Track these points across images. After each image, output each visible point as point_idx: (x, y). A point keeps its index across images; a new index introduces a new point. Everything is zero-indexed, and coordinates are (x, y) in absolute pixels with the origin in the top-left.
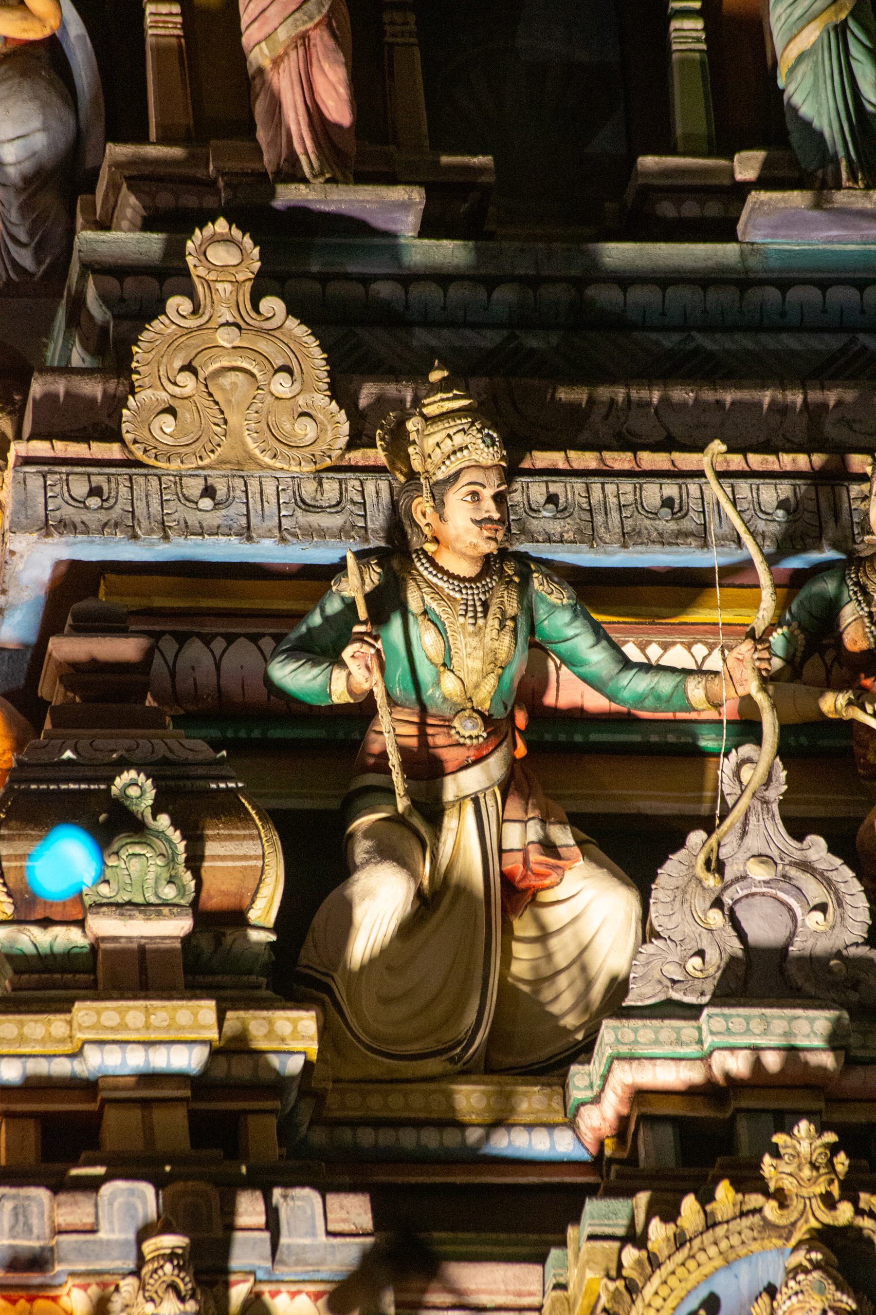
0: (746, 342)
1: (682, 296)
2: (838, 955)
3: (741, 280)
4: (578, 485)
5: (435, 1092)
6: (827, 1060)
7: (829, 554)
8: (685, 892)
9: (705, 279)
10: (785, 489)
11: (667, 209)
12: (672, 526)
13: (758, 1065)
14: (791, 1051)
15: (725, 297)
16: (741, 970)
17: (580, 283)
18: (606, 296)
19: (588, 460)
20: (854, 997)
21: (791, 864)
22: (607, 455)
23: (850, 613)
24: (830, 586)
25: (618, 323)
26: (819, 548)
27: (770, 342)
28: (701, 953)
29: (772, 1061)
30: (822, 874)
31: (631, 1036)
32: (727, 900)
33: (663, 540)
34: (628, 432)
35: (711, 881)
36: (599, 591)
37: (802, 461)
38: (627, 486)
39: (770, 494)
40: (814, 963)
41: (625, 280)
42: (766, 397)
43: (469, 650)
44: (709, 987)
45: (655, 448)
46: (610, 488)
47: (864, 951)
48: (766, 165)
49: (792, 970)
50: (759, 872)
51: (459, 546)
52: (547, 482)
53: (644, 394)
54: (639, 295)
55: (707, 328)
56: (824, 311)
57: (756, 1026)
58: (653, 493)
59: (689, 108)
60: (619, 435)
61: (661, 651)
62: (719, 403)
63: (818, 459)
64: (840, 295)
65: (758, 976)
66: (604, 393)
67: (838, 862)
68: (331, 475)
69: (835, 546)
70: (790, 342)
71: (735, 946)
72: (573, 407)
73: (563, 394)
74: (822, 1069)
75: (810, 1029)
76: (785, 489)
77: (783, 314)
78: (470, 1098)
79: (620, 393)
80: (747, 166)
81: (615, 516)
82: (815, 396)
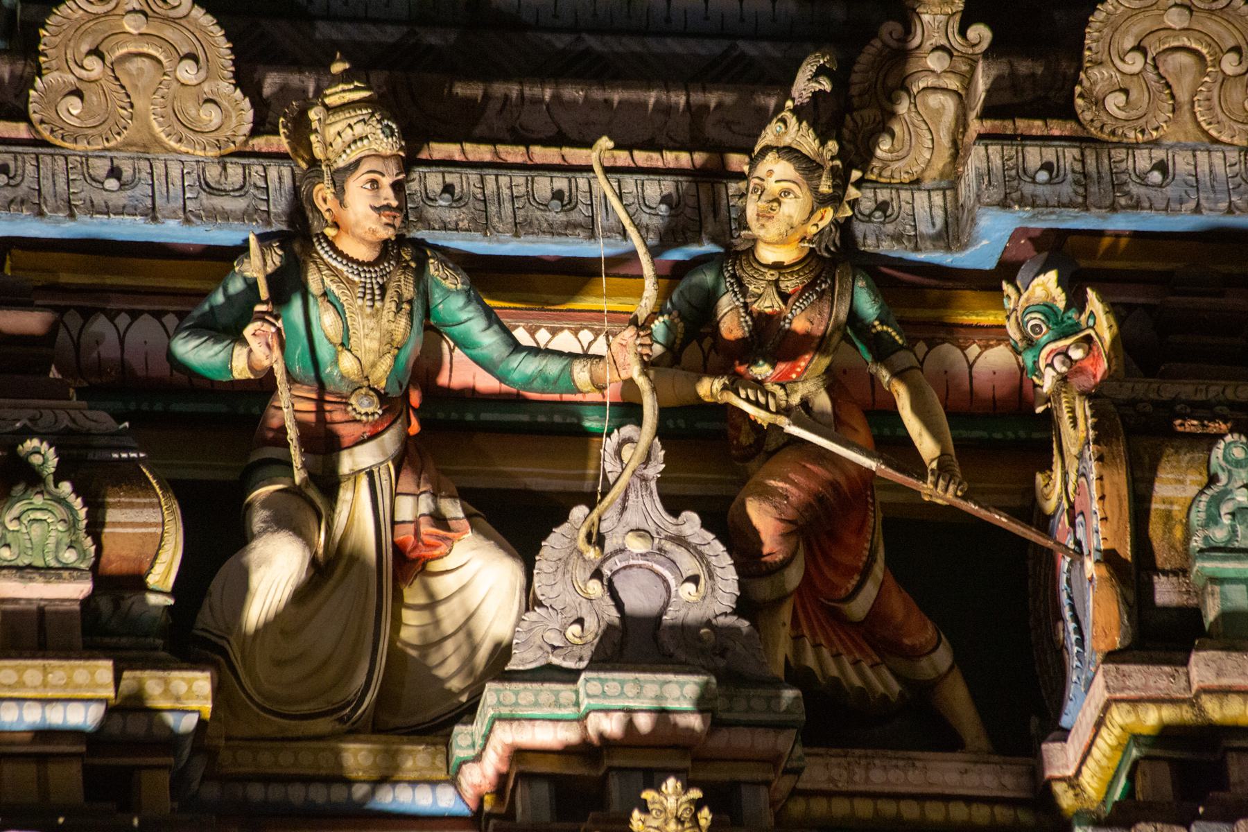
0: (633, 45)
2: (708, 624)
4: (474, 176)
5: (323, 750)
6: (695, 722)
7: (708, 248)
8: (566, 564)
10: (668, 185)
12: (562, 217)
13: (630, 726)
14: (662, 713)
16: (617, 637)
19: (482, 152)
20: (722, 663)
21: (666, 538)
22: (500, 148)
23: (726, 303)
24: (709, 278)
26: (699, 241)
28: (580, 621)
29: (644, 722)
30: (695, 548)
31: (511, 698)
32: (606, 572)
33: (553, 231)
34: (521, 126)
35: (592, 553)
36: (491, 278)
37: (684, 159)
38: (519, 179)
39: (654, 190)
40: (685, 631)
42: (652, 97)
43: (367, 331)
44: (587, 653)
45: (546, 143)
46: (504, 180)
47: (732, 620)
49: (665, 637)
50: (637, 546)
51: (359, 231)
52: (443, 173)
53: (537, 91)
57: (630, 690)
58: (544, 185)
60: (512, 130)
61: (549, 336)
62: (607, 102)
63: (699, 157)
65: (634, 643)
66: (498, 89)
67: (710, 536)
68: (235, 160)
69: (714, 240)
71: (613, 614)
72: (469, 102)
73: (460, 90)
74: (690, 730)
75: (680, 692)
76: (668, 185)
77: (668, 20)
78: (357, 756)
79: (514, 90)
81: (507, 206)
82: (697, 98)
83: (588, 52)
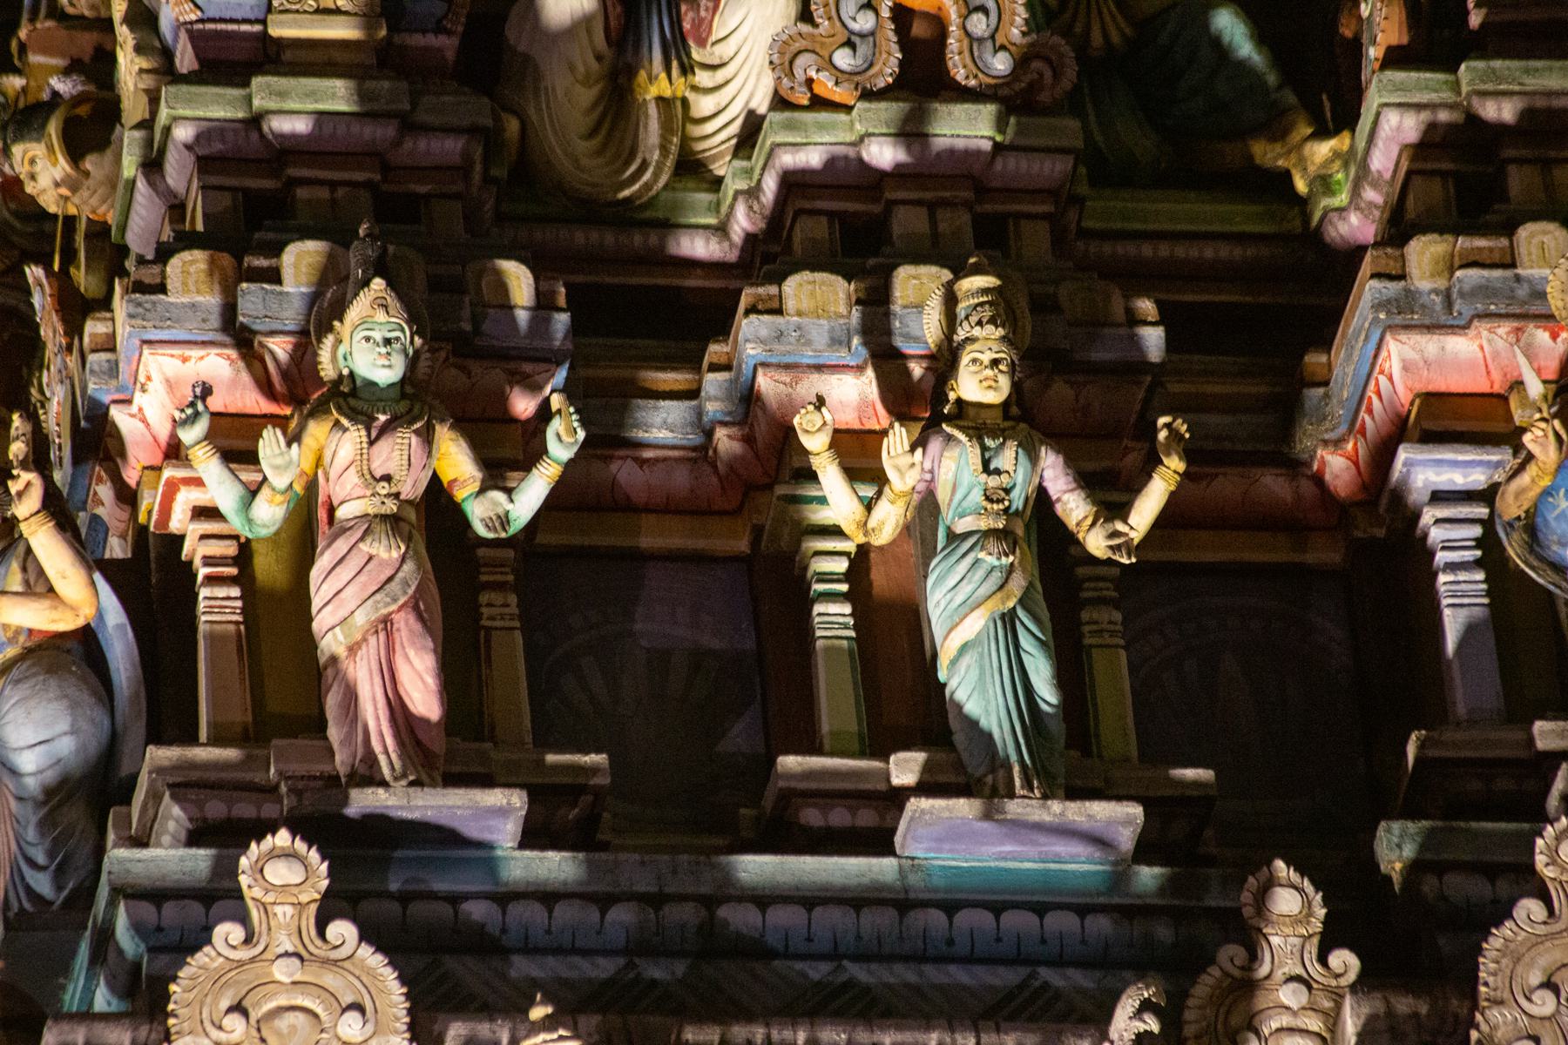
0: (906, 974)
1: (831, 919)
3: (901, 901)
9: (857, 899)
11: (812, 817)
15: (877, 921)
17: (710, 902)
18: (741, 918)
25: (755, 950)
27: (933, 974)
41: (764, 899)
48: (927, 768)
53: (787, 1034)
54: (782, 916)
55: (861, 958)
56: (999, 940)
59: (836, 699)
64: (1014, 921)
70: (959, 975)
77: (950, 942)
80: (905, 768)
83: (850, 984)
